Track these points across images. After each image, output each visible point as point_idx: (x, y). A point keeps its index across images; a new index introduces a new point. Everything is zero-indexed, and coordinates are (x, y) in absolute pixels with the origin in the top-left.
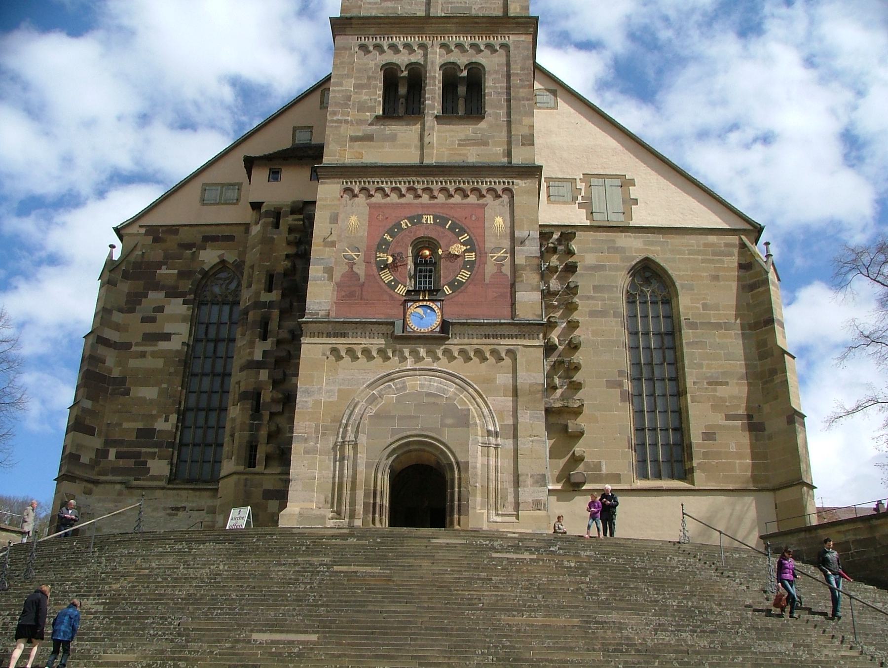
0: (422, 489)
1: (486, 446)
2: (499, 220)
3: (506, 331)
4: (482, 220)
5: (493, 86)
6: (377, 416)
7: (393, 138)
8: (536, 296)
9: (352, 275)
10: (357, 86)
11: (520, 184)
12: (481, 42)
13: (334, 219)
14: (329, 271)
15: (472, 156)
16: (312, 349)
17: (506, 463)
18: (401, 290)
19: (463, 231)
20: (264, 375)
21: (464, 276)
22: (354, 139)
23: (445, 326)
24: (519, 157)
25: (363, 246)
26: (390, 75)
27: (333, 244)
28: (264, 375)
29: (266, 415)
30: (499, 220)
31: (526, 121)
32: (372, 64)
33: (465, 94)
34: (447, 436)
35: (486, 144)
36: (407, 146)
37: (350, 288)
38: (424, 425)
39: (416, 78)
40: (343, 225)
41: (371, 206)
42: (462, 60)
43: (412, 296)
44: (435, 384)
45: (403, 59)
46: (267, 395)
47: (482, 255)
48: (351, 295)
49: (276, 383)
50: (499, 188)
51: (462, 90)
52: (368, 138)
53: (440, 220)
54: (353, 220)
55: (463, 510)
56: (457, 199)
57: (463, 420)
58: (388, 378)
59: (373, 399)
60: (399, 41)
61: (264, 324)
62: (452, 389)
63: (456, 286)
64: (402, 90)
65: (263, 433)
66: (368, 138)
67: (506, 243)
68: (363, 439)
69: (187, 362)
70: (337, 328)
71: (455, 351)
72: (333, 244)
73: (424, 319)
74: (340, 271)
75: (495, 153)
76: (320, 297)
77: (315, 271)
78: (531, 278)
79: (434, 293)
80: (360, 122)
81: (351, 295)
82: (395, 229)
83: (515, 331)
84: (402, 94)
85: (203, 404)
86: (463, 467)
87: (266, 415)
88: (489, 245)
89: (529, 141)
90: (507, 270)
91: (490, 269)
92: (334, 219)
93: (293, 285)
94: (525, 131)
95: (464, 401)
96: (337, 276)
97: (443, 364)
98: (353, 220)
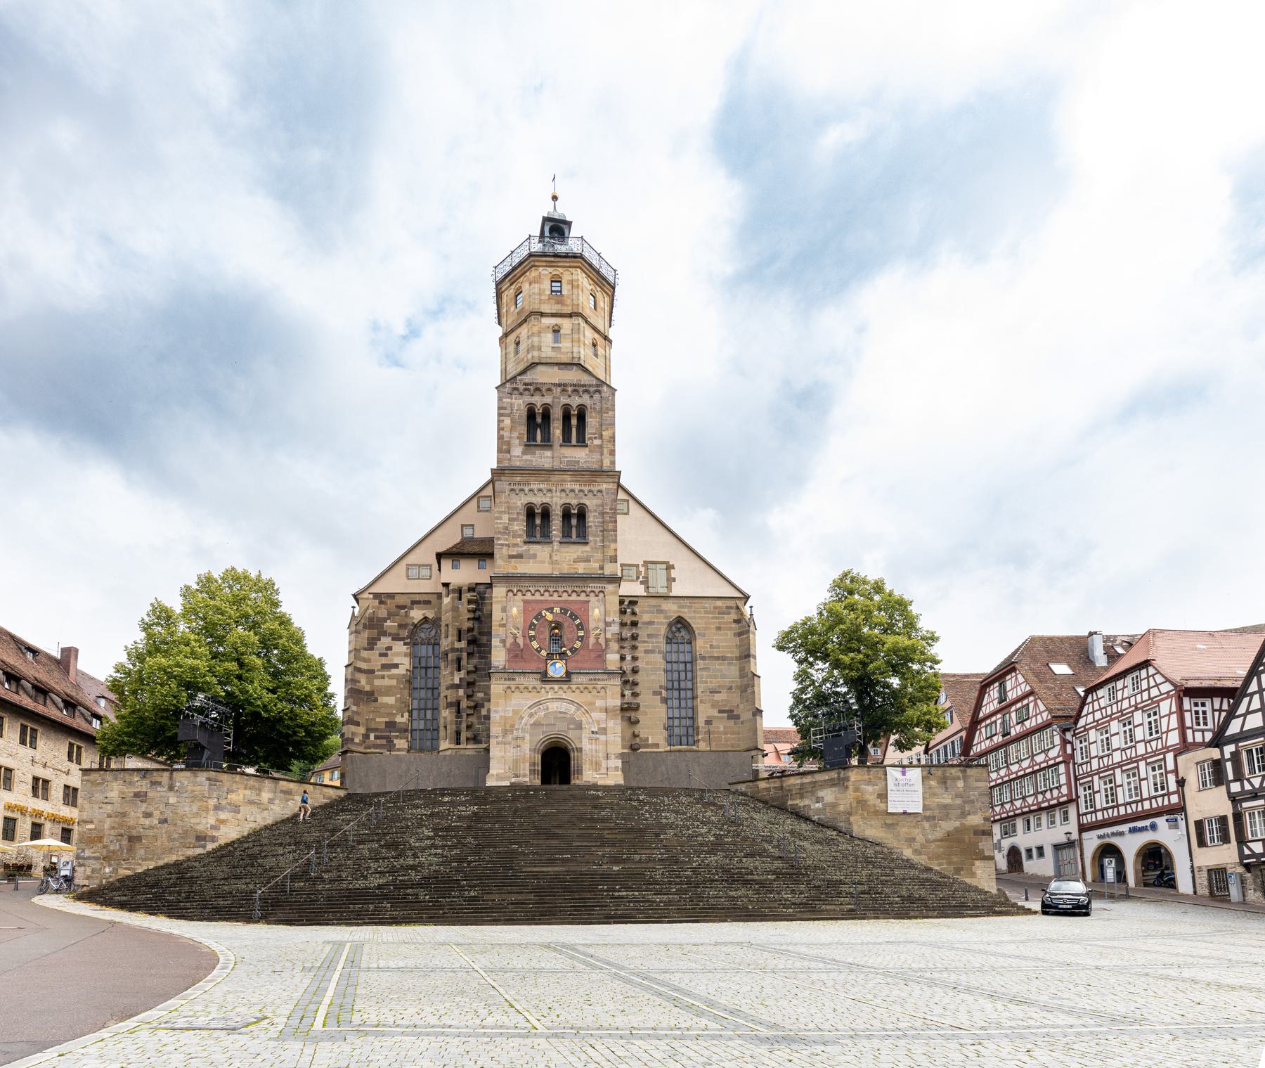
0: (556, 761)
1: (591, 739)
2: (597, 611)
3: (600, 677)
4: (587, 610)
5: (592, 520)
6: (534, 724)
7: (534, 556)
8: (617, 657)
9: (515, 644)
10: (510, 520)
11: (610, 588)
12: (586, 489)
13: (504, 610)
14: (503, 642)
15: (581, 569)
16: (497, 687)
17: (601, 747)
18: (544, 653)
19: (577, 618)
20: (461, 692)
21: (578, 644)
22: (511, 557)
23: (568, 674)
24: (609, 569)
25: (521, 626)
26: (530, 513)
27: (504, 625)
28: (461, 692)
29: (464, 715)
30: (597, 611)
31: (613, 546)
32: (519, 503)
33: (575, 520)
34: (571, 734)
35: (589, 561)
36: (543, 562)
37: (516, 653)
38: (559, 729)
39: (546, 514)
40: (508, 612)
41: (525, 602)
42: (574, 502)
43: (550, 657)
44: (564, 707)
45: (538, 500)
46: (464, 704)
47: (587, 632)
48: (516, 656)
49: (469, 697)
50: (597, 591)
51: (574, 522)
52: (520, 556)
53: (564, 611)
54: (515, 610)
55: (580, 772)
56: (574, 597)
57: (579, 726)
58: (539, 703)
59: (531, 715)
60: (535, 487)
61: (459, 660)
62: (572, 708)
63: (574, 650)
64: (538, 521)
65: (464, 726)
66: (520, 556)
67: (601, 625)
68: (527, 737)
69: (409, 681)
70: (509, 675)
71: (574, 687)
72: (504, 625)
73: (557, 669)
74: (510, 641)
75: (593, 567)
76: (499, 657)
77: (495, 642)
78: (614, 646)
79: (562, 656)
80: (516, 545)
81: (516, 656)
82: (539, 616)
83: (605, 677)
84: (537, 519)
85: (422, 706)
86: (580, 750)
87: (464, 715)
88: (592, 625)
89: (614, 559)
90: (602, 641)
91: (592, 640)
92: (504, 610)
93: (477, 639)
94: (612, 553)
95: (579, 716)
96: (508, 645)
97: (569, 696)
98: (515, 610)
